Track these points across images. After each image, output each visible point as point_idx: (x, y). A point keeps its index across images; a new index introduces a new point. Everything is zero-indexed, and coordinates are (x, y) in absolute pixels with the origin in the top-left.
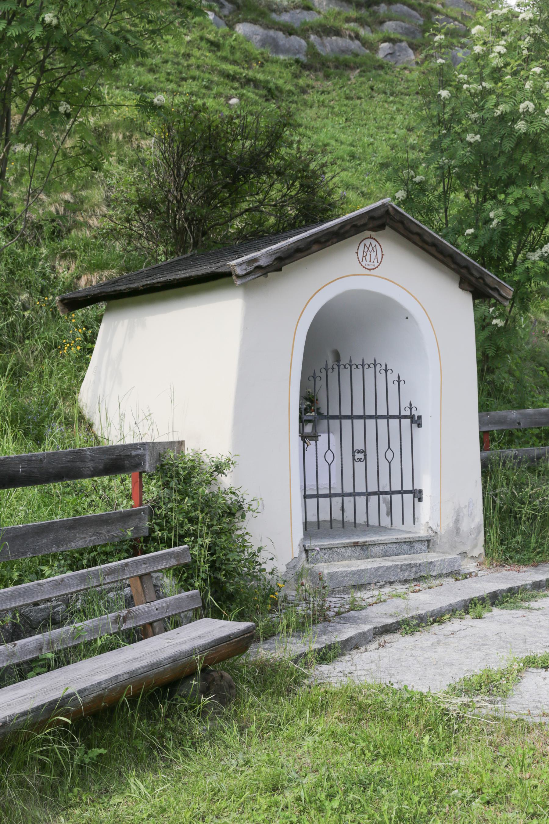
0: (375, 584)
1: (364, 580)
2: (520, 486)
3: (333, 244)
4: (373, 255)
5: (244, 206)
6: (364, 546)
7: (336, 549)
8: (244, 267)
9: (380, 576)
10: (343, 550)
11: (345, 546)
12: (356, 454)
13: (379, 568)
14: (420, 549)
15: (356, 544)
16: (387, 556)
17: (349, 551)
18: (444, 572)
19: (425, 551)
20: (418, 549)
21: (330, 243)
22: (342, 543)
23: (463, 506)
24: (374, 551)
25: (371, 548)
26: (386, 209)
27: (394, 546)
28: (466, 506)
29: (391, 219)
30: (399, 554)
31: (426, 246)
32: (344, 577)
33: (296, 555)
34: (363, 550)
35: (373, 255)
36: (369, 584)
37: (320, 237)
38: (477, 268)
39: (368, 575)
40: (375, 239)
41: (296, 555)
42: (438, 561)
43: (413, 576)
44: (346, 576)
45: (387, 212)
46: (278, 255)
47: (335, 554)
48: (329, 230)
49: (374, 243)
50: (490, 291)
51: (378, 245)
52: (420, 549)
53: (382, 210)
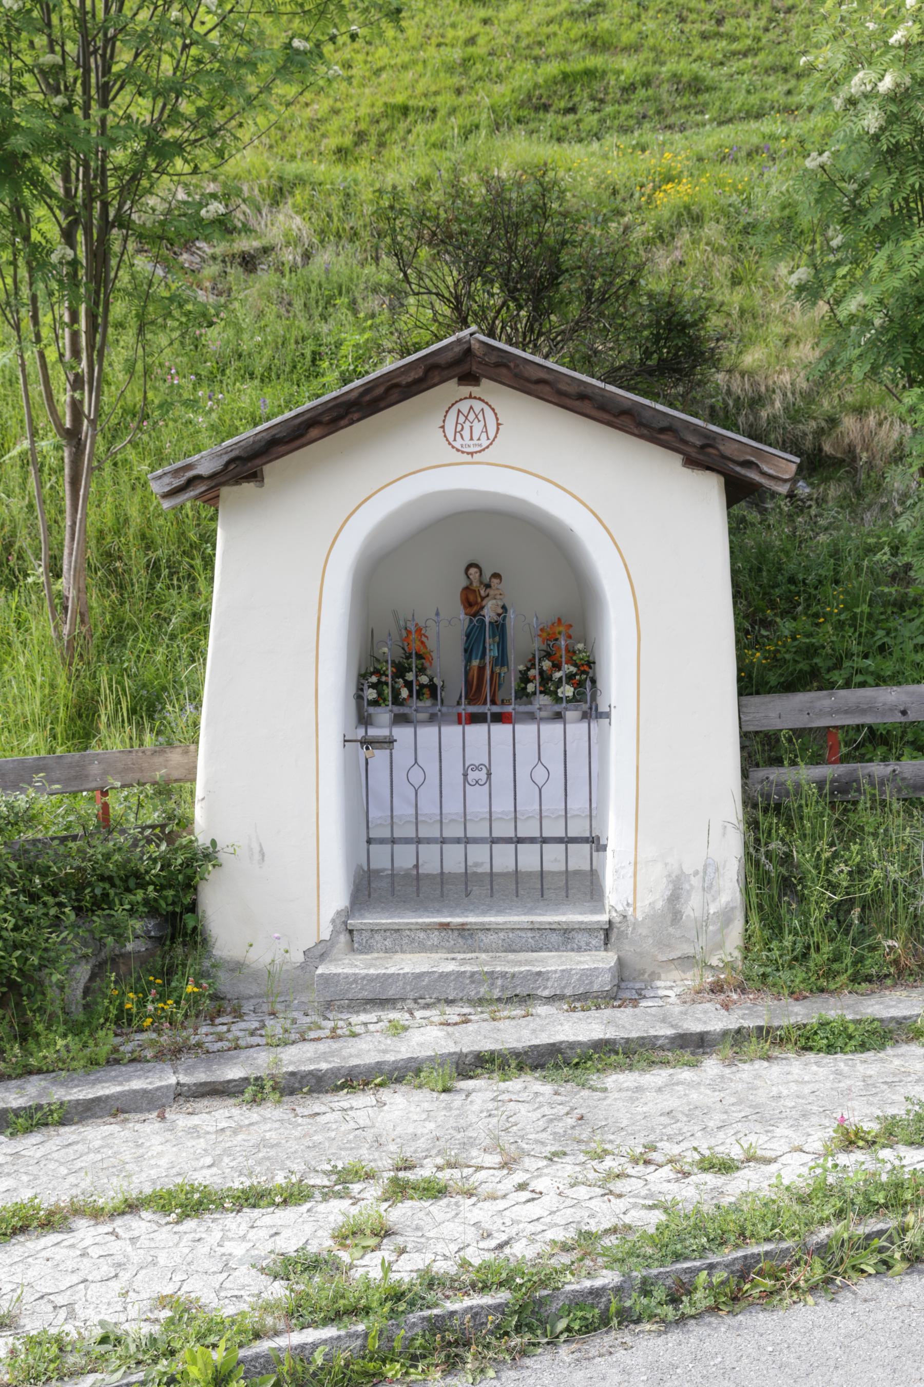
0: (415, 1001)
1: (390, 993)
2: (875, 835)
3: (352, 422)
4: (478, 427)
5: (499, 331)
6: (462, 929)
7: (408, 933)
8: (166, 480)
9: (426, 988)
10: (422, 935)
11: (426, 928)
12: (470, 771)
13: (422, 974)
14: (588, 944)
15: (445, 927)
16: (514, 951)
17: (435, 938)
18: (568, 992)
19: (597, 949)
20: (583, 944)
21: (343, 423)
22: (417, 923)
23: (688, 870)
24: (486, 941)
25: (480, 934)
26: (466, 346)
27: (530, 934)
28: (696, 873)
29: (480, 363)
30: (540, 950)
31: (568, 402)
32: (351, 983)
33: (326, 935)
34: (463, 937)
35: (478, 427)
36: (404, 1000)
37: (321, 414)
38: (696, 429)
39: (401, 983)
40: (480, 399)
41: (326, 935)
42: (555, 972)
43: (497, 993)
44: (355, 981)
45: (468, 352)
46: (233, 454)
47: (406, 940)
48: (339, 401)
49: (478, 406)
50: (738, 469)
51: (487, 409)
52: (588, 944)
53: (457, 349)
